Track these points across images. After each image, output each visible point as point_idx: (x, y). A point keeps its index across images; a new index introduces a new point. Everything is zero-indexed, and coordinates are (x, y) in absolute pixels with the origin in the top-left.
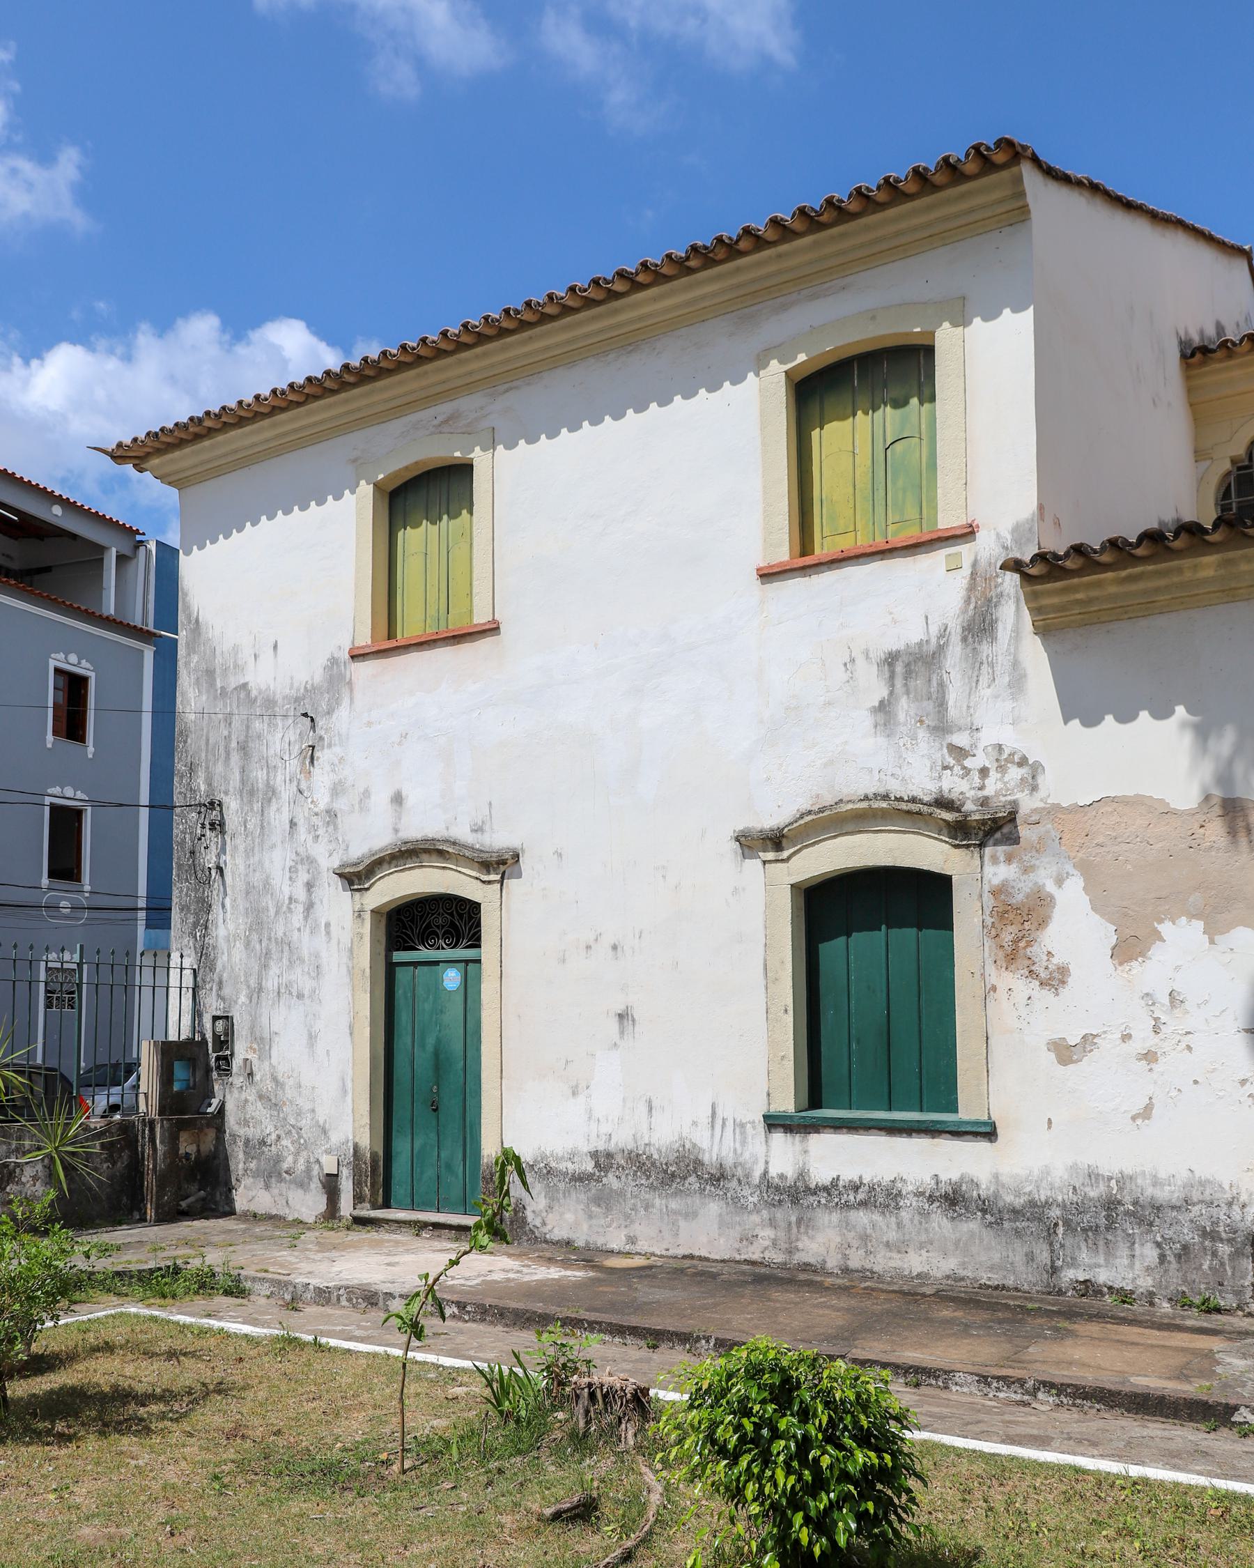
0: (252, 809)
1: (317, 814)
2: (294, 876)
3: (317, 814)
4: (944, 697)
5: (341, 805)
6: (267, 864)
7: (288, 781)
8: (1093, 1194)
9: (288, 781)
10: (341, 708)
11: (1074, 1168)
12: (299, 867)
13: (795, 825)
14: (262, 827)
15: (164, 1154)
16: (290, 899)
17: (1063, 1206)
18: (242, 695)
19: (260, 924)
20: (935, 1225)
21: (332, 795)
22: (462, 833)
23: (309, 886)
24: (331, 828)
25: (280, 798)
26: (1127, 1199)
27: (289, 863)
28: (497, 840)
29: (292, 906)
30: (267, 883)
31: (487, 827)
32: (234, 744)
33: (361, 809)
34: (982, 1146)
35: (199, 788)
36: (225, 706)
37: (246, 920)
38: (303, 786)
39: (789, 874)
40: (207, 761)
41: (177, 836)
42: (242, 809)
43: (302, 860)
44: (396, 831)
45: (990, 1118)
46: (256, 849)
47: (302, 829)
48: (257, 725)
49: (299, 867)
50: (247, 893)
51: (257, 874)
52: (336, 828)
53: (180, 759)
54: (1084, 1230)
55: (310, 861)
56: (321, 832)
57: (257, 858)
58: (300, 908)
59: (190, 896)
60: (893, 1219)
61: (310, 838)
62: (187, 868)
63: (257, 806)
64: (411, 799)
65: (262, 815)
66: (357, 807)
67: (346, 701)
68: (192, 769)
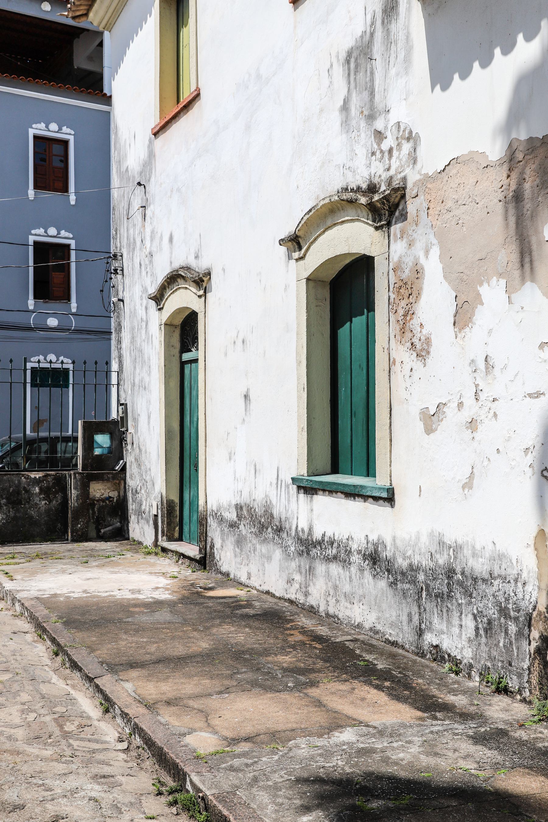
4: (373, 84)
8: (441, 562)
11: (431, 534)
13: (300, 225)
15: (77, 496)
17: (425, 571)
20: (366, 581)
26: (458, 569)
34: (388, 509)
39: (305, 270)
45: (391, 485)
54: (437, 596)
60: (348, 573)
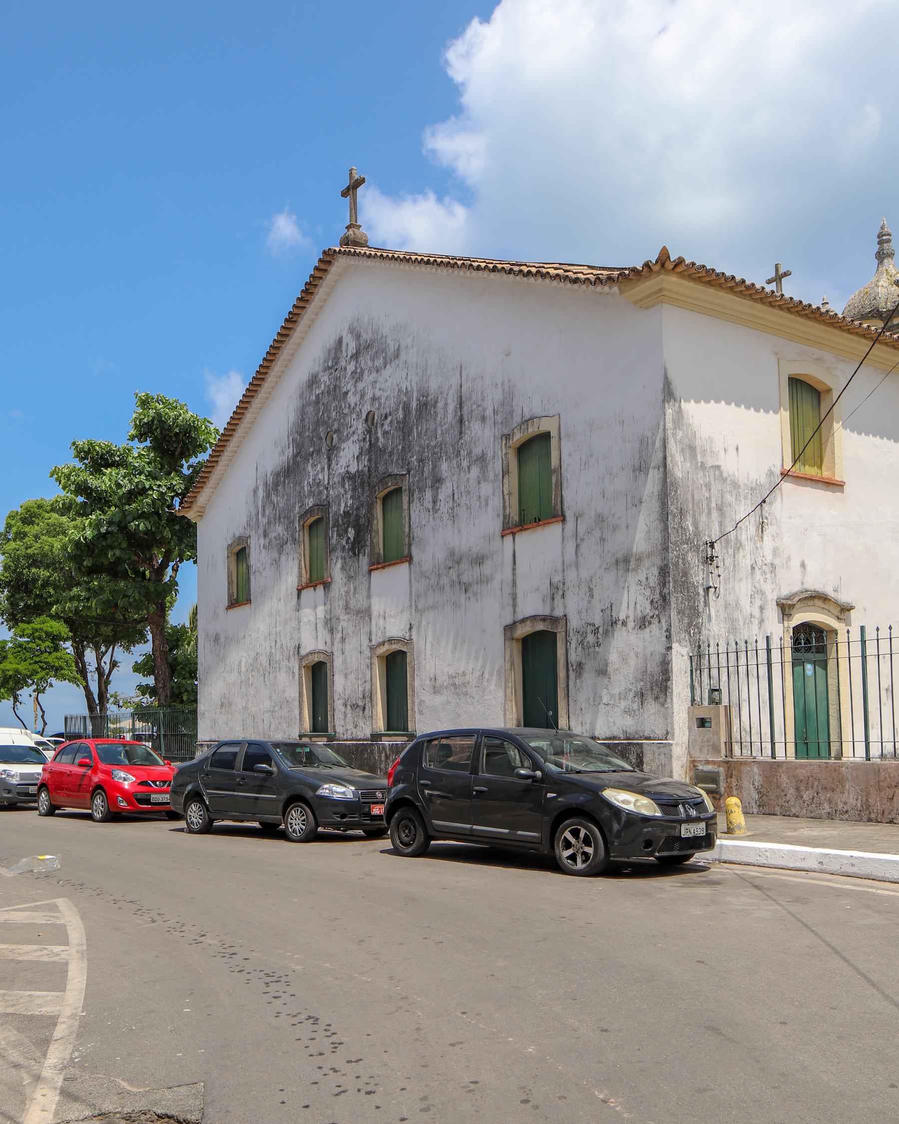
0: (728, 552)
1: (766, 565)
2: (753, 601)
3: (766, 565)
5: (777, 562)
6: (737, 591)
7: (749, 540)
9: (749, 540)
10: (777, 503)
12: (756, 595)
14: (734, 566)
16: (751, 615)
18: (717, 473)
19: (735, 629)
21: (773, 555)
22: (829, 591)
23: (762, 608)
24: (773, 575)
25: (745, 549)
27: (750, 593)
28: (844, 597)
29: (752, 620)
30: (737, 604)
31: (839, 590)
32: (713, 505)
33: (787, 567)
35: (688, 528)
36: (705, 476)
37: (725, 625)
38: (758, 545)
40: (694, 511)
41: (672, 559)
42: (721, 550)
43: (758, 591)
44: (803, 583)
46: (731, 579)
47: (758, 572)
48: (728, 497)
49: (756, 595)
50: (726, 608)
51: (732, 596)
52: (775, 576)
53: (672, 503)
55: (762, 593)
56: (768, 576)
57: (731, 585)
58: (756, 622)
59: (685, 604)
61: (762, 582)
62: (681, 583)
63: (731, 551)
64: (809, 568)
65: (734, 558)
66: (785, 565)
67: (779, 499)
68: (682, 513)
